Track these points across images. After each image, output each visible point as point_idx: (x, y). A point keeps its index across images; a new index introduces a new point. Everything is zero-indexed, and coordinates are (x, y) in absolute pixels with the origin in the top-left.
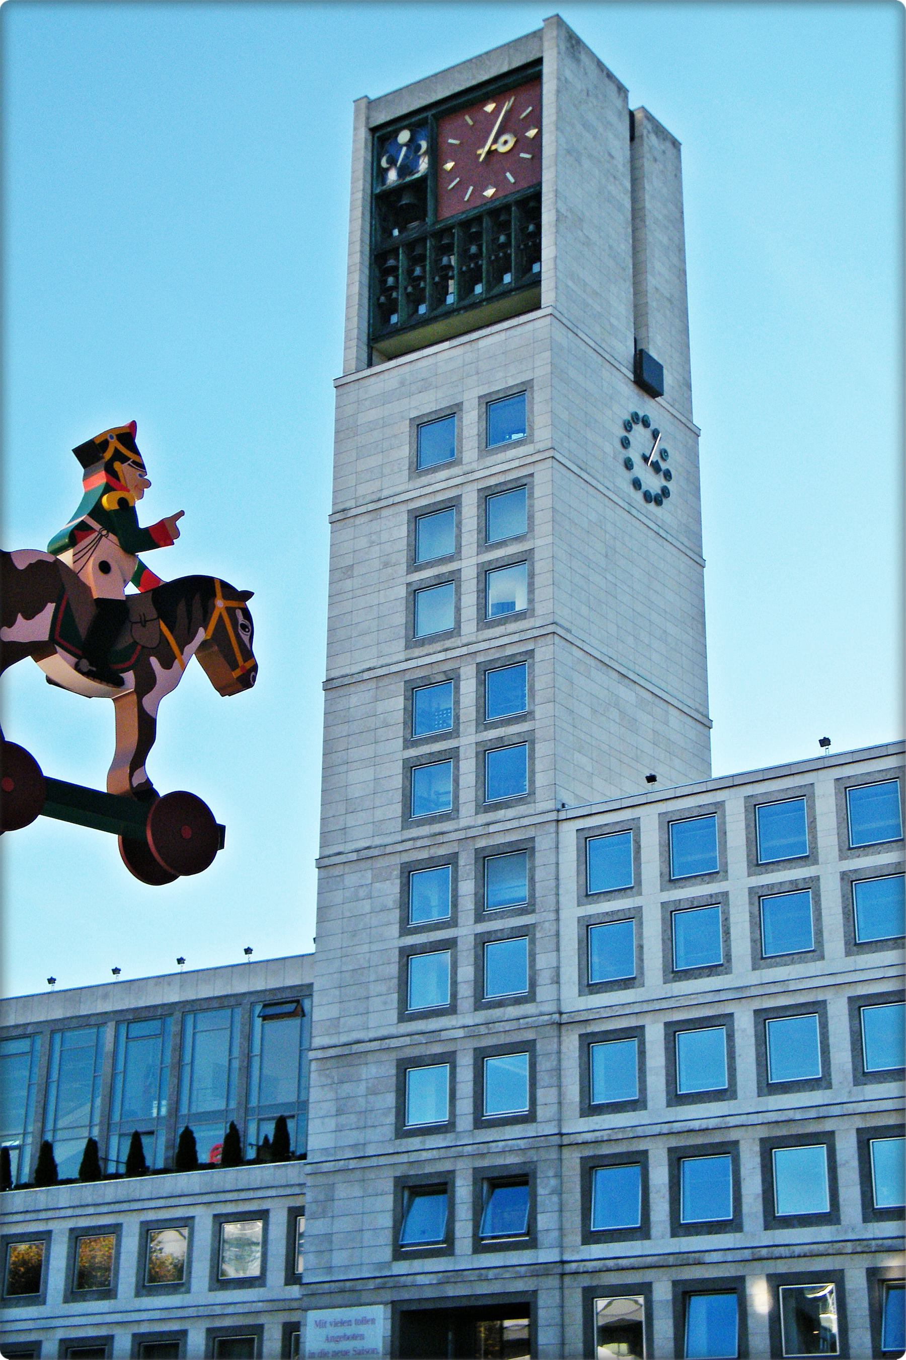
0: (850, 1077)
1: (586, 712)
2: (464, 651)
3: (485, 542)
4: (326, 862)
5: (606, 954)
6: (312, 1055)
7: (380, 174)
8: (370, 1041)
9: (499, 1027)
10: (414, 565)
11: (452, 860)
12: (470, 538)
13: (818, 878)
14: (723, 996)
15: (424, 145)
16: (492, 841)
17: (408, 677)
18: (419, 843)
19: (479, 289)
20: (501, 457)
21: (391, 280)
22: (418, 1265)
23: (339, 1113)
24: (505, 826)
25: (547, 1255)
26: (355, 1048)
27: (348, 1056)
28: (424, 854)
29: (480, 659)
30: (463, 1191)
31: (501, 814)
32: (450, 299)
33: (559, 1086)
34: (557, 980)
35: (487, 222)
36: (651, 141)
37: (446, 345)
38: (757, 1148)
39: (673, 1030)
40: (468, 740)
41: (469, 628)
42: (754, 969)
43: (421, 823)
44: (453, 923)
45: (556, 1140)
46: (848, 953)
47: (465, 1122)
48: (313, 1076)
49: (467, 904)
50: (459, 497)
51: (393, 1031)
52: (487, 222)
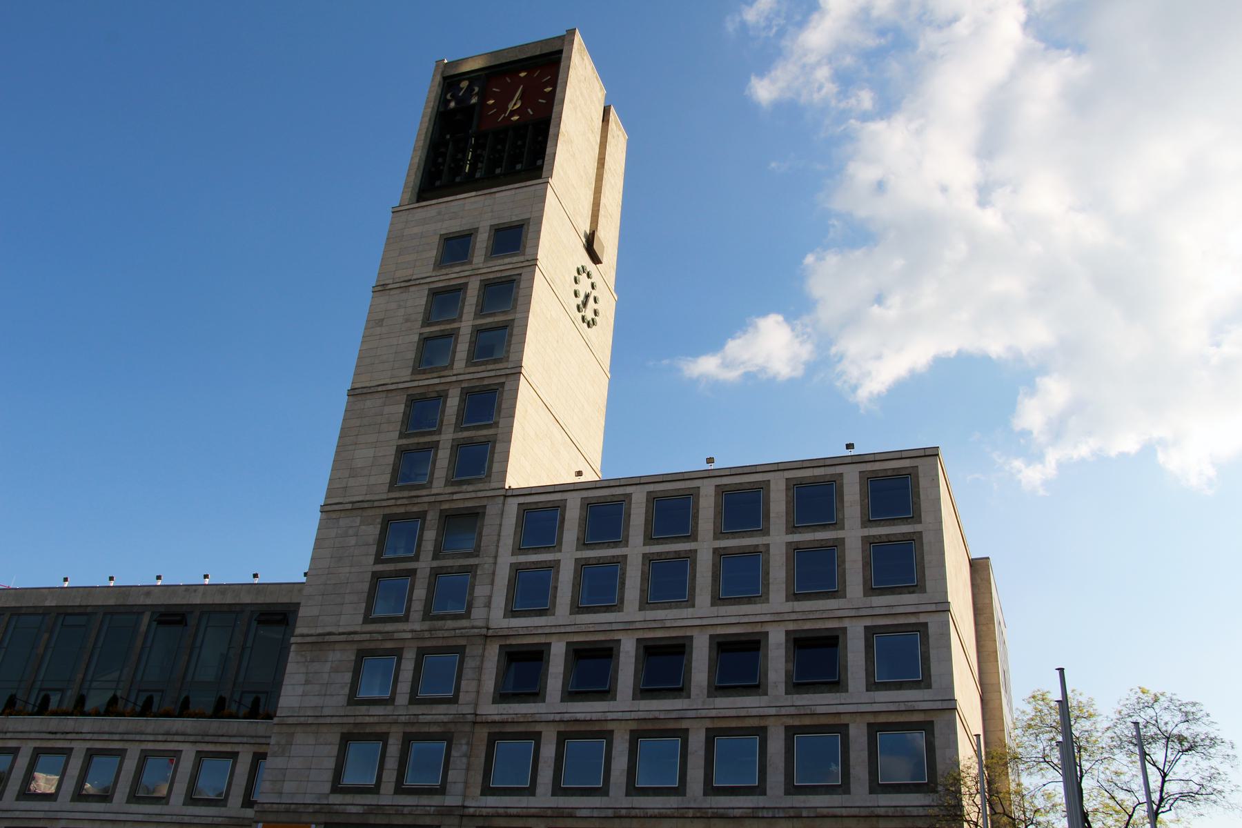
0: (705, 691)
2: (454, 378)
4: (329, 508)
5: (530, 590)
6: (293, 640)
7: (443, 101)
8: (340, 634)
9: (440, 634)
11: (422, 515)
13: (696, 551)
14: (615, 627)
15: (477, 89)
16: (454, 505)
17: (410, 392)
18: (399, 502)
20: (501, 262)
21: (440, 160)
22: (348, 799)
23: (307, 682)
24: (465, 496)
25: (449, 801)
26: (327, 638)
27: (321, 643)
28: (402, 510)
29: (465, 385)
32: (478, 175)
33: (479, 680)
34: (488, 605)
37: (473, 194)
38: (627, 737)
40: (447, 437)
42: (640, 610)
43: (402, 489)
44: (416, 558)
45: (470, 718)
46: (713, 605)
47: (402, 698)
48: (292, 655)
50: (466, 284)
51: (358, 629)
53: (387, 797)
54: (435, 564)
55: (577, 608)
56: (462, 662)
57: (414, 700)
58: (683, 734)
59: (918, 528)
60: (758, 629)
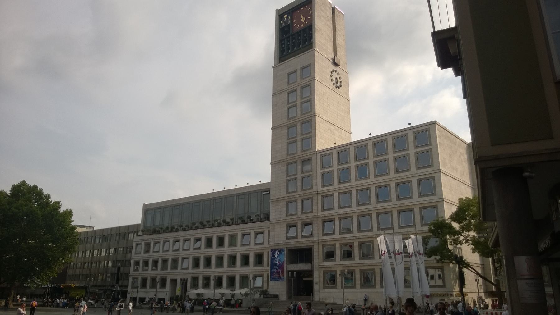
1: (323, 131)
3: (302, 98)
5: (326, 179)
10: (288, 103)
11: (296, 162)
12: (299, 97)
19: (301, 46)
22: (291, 241)
25: (315, 238)
27: (277, 201)
30: (299, 226)
31: (306, 152)
35: (302, 32)
36: (337, 13)
39: (340, 194)
40: (299, 138)
41: (299, 115)
44: (296, 174)
47: (299, 213)
49: (299, 171)
52: (302, 32)
53: (299, 239)
54: (302, 175)
55: (340, 183)
56: (312, 202)
57: (302, 213)
58: (370, 215)
59: (430, 147)
60: (387, 183)
